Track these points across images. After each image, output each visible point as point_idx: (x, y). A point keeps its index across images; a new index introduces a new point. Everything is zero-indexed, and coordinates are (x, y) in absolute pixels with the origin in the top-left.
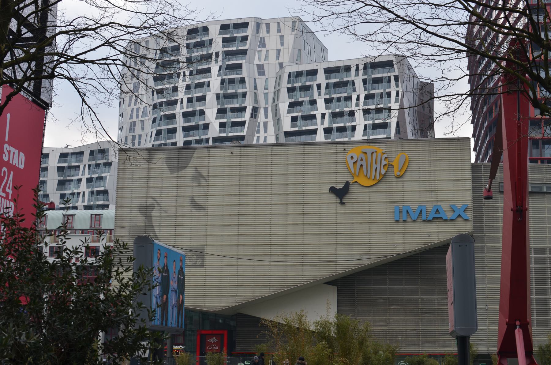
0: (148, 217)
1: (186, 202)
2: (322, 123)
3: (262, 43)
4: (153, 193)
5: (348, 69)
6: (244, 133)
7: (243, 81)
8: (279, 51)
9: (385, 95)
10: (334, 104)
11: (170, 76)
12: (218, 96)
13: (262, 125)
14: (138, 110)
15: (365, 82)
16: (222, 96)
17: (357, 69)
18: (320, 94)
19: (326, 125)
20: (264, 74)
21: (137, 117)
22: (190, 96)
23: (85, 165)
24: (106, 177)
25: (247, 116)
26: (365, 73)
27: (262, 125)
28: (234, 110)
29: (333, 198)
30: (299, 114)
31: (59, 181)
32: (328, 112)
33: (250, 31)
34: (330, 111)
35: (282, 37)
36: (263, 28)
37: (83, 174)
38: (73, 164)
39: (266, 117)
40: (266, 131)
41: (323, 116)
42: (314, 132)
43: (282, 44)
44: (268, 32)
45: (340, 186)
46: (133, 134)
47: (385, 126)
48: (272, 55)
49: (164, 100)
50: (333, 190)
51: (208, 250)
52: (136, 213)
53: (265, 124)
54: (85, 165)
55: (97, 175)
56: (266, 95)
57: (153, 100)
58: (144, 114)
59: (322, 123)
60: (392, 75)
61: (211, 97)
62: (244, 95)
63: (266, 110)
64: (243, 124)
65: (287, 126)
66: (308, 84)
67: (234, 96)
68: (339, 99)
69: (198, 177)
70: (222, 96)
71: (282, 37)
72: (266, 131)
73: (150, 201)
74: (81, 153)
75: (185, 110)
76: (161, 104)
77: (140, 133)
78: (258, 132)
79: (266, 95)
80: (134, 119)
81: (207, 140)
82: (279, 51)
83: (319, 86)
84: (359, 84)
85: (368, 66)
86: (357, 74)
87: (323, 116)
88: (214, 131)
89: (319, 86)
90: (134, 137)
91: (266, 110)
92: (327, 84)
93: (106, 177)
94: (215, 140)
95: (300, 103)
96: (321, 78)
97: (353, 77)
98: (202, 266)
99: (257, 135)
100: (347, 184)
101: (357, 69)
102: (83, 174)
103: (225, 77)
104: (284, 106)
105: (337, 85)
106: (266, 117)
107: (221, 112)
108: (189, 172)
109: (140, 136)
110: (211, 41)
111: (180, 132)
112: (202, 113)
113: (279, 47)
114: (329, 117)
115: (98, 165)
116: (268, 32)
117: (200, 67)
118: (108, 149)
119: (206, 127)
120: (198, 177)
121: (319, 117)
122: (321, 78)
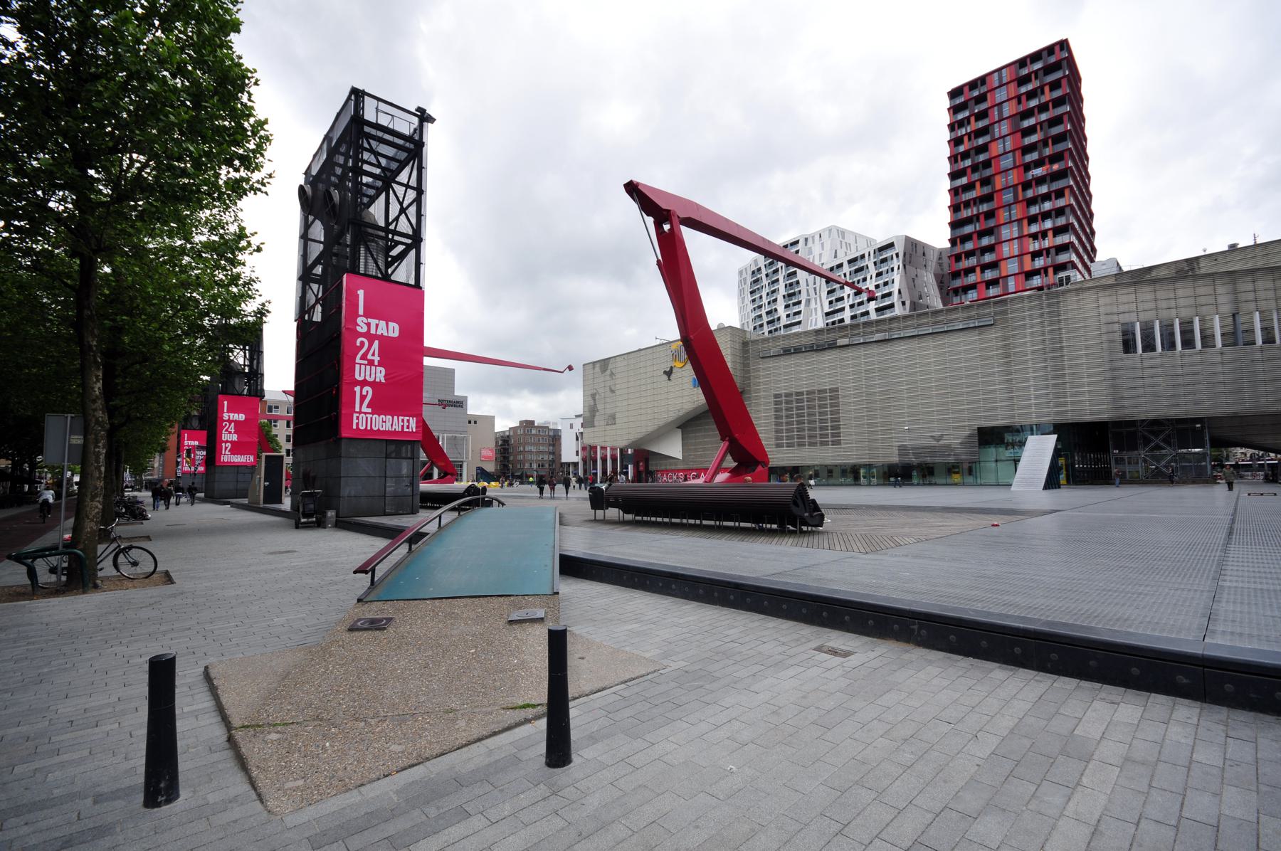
0: (595, 400)
1: (608, 389)
4: (596, 387)
5: (863, 257)
7: (798, 282)
8: (821, 255)
12: (784, 296)
19: (851, 303)
26: (875, 257)
28: (795, 304)
29: (665, 377)
33: (800, 246)
35: (822, 244)
36: (810, 241)
39: (816, 304)
40: (816, 314)
41: (849, 296)
42: (843, 309)
44: (813, 243)
45: (668, 370)
50: (665, 372)
51: (617, 416)
53: (816, 309)
61: (780, 298)
62: (800, 292)
65: (827, 309)
67: (794, 294)
71: (822, 244)
75: (767, 310)
82: (821, 255)
88: (784, 321)
100: (672, 367)
104: (824, 294)
105: (857, 271)
106: (816, 304)
107: (787, 306)
108: (608, 372)
112: (776, 310)
113: (821, 252)
116: (813, 243)
120: (612, 374)
121: (846, 298)
122: (846, 269)
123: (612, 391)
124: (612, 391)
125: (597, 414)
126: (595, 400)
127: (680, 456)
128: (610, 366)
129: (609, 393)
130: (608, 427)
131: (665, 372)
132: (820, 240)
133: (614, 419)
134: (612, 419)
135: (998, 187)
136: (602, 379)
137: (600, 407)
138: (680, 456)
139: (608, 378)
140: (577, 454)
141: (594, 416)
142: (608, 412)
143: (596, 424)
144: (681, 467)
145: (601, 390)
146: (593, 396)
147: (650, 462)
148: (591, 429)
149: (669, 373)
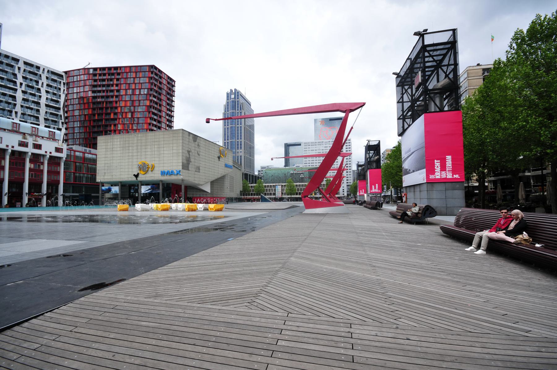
0: (189, 155)
18: (19, 72)
19: (23, 88)
29: (217, 159)
30: (5, 77)
34: (26, 83)
41: (21, 84)
51: (201, 168)
52: (186, 152)
59: (21, 87)
68: (31, 80)
69: (198, 145)
73: (189, 150)
83: (19, 68)
87: (21, 84)
96: (20, 64)
98: (199, 172)
105: (30, 72)
108: (196, 143)
114: (25, 86)
124: (199, 155)
125: (191, 163)
127: (209, 191)
128: (198, 141)
129: (196, 155)
130: (196, 173)
131: (218, 157)
134: (198, 169)
135: (122, 94)
136: (193, 145)
137: (192, 160)
138: (209, 191)
139: (196, 146)
141: (189, 164)
142: (197, 164)
143: (190, 168)
144: (209, 196)
145: (193, 151)
146: (189, 152)
147: (188, 193)
148: (187, 171)
149: (219, 158)
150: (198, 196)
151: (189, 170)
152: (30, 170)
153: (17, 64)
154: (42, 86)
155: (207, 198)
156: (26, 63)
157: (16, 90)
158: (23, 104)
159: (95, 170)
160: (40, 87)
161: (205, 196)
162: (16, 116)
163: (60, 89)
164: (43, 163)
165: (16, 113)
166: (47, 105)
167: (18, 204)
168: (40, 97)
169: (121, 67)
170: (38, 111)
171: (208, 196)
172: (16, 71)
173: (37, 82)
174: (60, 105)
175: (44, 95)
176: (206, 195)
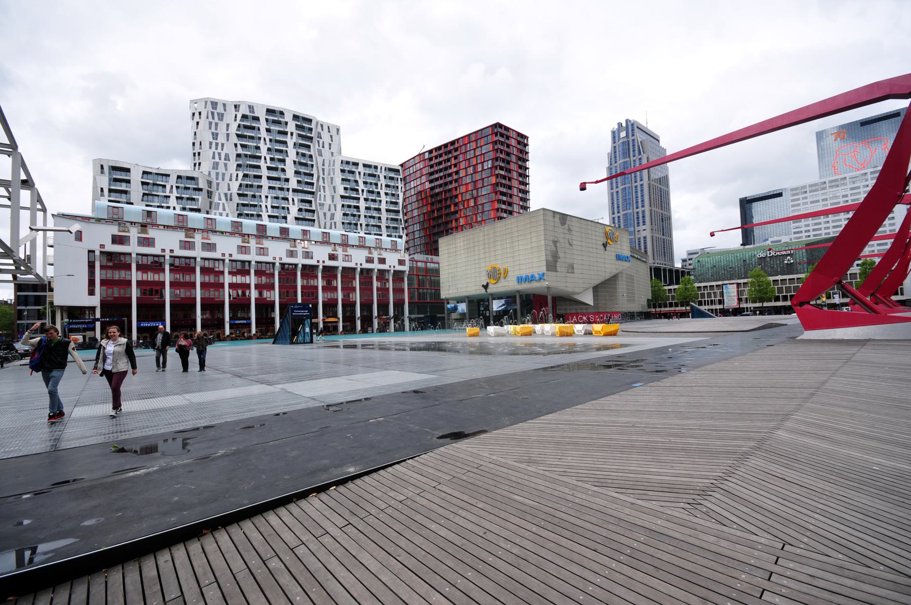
0: (556, 247)
2: (363, 195)
3: (319, 136)
6: (314, 190)
8: (330, 145)
9: (395, 187)
10: (368, 185)
11: (252, 138)
12: (295, 162)
13: (322, 187)
14: (219, 154)
15: (385, 177)
16: (297, 163)
17: (381, 169)
18: (360, 178)
20: (322, 156)
21: (220, 159)
22: (272, 156)
23: (172, 186)
24: (198, 199)
25: (314, 181)
27: (322, 187)
28: (305, 174)
29: (602, 247)
31: (144, 194)
32: (365, 189)
35: (331, 136)
37: (171, 192)
38: (158, 183)
39: (324, 183)
40: (324, 192)
41: (363, 191)
43: (332, 141)
46: (217, 171)
47: (396, 203)
48: (327, 146)
49: (250, 153)
51: (575, 266)
52: (551, 244)
53: (324, 187)
54: (172, 186)
55: (188, 196)
56: (323, 170)
57: (236, 150)
58: (227, 158)
59: (363, 195)
60: (399, 177)
61: (289, 161)
63: (323, 179)
64: (312, 184)
66: (353, 170)
68: (371, 184)
69: (569, 230)
70: (297, 163)
71: (331, 136)
72: (324, 192)
73: (556, 239)
74: (169, 175)
76: (246, 156)
77: (224, 171)
78: (320, 191)
79: (323, 170)
80: (217, 159)
81: (288, 190)
82: (330, 145)
83: (359, 173)
84: (382, 177)
85: (344, 163)
86: (381, 172)
87: (363, 191)
88: (293, 184)
89: (359, 173)
90: (217, 174)
91: (323, 179)
92: (364, 173)
93: (198, 199)
94: (294, 191)
95: (349, 180)
96: (361, 168)
97: (378, 173)
99: (319, 193)
101: (381, 169)
102: (171, 192)
103: (298, 151)
105: (370, 175)
106: (324, 183)
107: (297, 173)
108: (566, 226)
109: (223, 175)
110: (286, 123)
111: (264, 179)
115: (187, 188)
116: (322, 130)
117: (277, 138)
118: (198, 178)
119: (287, 180)
123: (571, 245)
124: (571, 245)
125: (559, 260)
126: (556, 247)
127: (591, 303)
128: (568, 222)
129: (567, 245)
130: (569, 275)
131: (603, 244)
132: (329, 132)
133: (573, 268)
134: (571, 268)
135: (461, 176)
137: (561, 255)
138: (591, 303)
139: (566, 231)
140: (91, 292)
143: (558, 269)
145: (561, 240)
146: (555, 242)
147: (557, 307)
148: (554, 274)
149: (605, 245)
150: (574, 311)
151: (557, 271)
152: (378, 289)
153: (357, 168)
154: (381, 189)
155: (589, 314)
156: (365, 166)
157: (358, 199)
158: (366, 214)
159: (438, 283)
160: (379, 190)
161: (584, 311)
162: (362, 230)
163: (397, 187)
164: (388, 280)
165: (361, 225)
166: (387, 211)
167: (370, 329)
168: (380, 201)
169: (458, 140)
170: (380, 218)
171: (590, 311)
172: (358, 178)
173: (376, 185)
174: (399, 207)
175: (384, 198)
176: (587, 309)
